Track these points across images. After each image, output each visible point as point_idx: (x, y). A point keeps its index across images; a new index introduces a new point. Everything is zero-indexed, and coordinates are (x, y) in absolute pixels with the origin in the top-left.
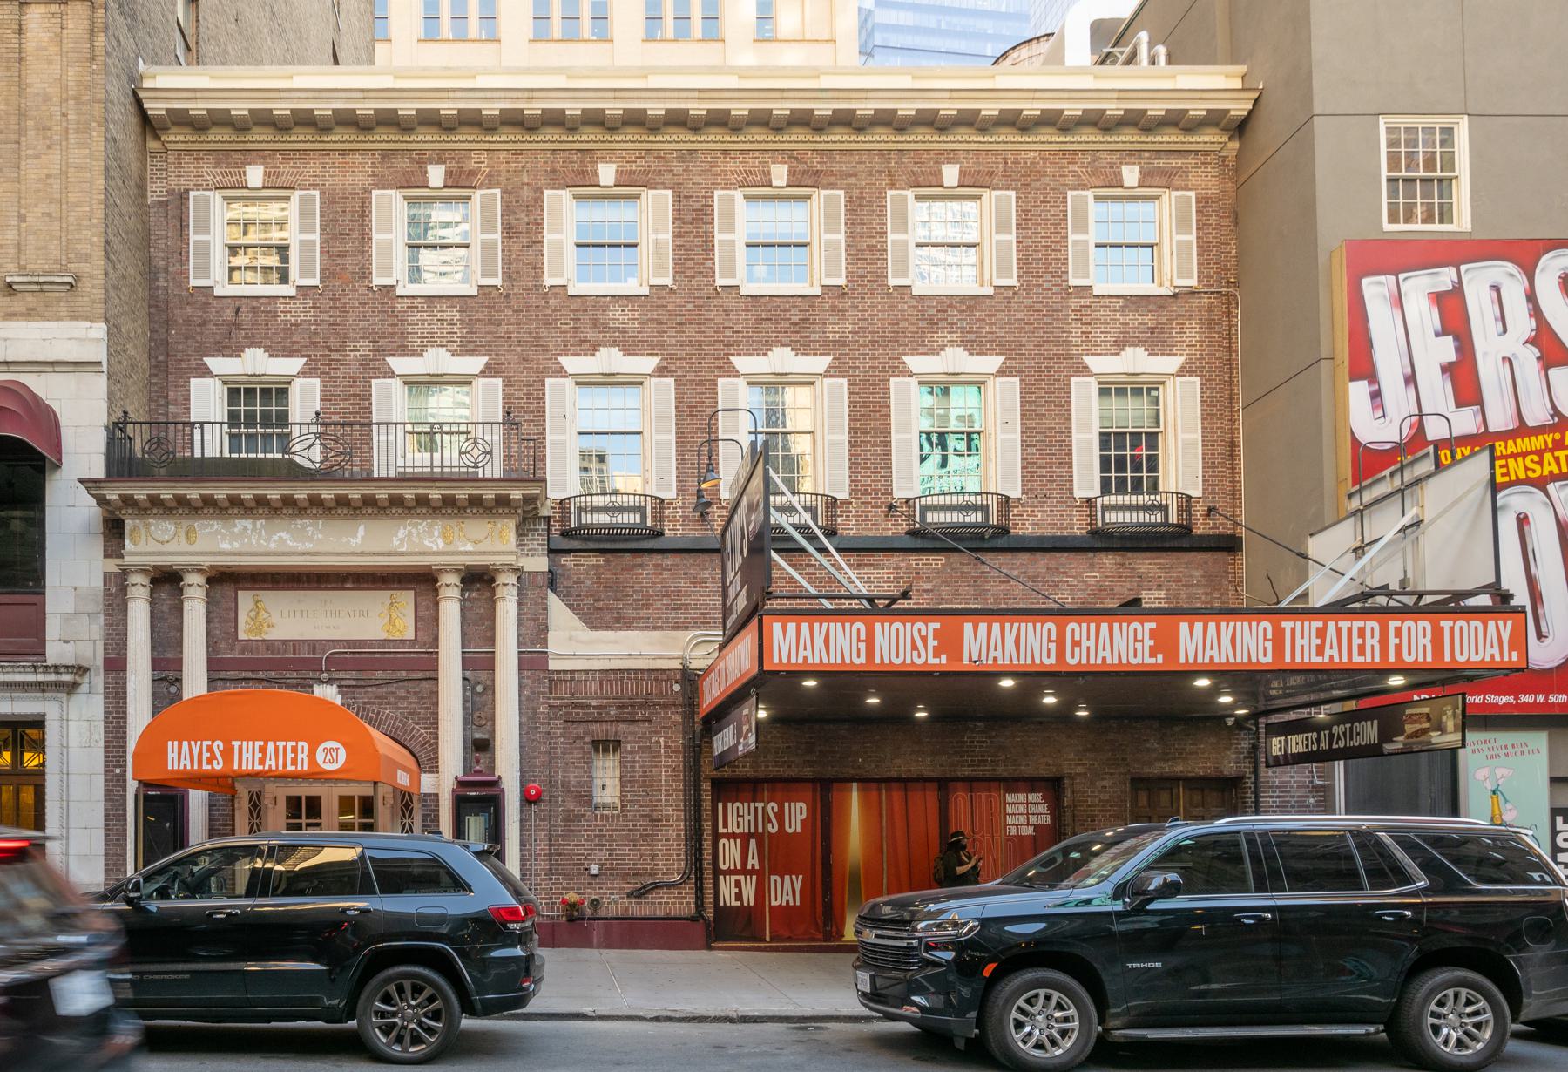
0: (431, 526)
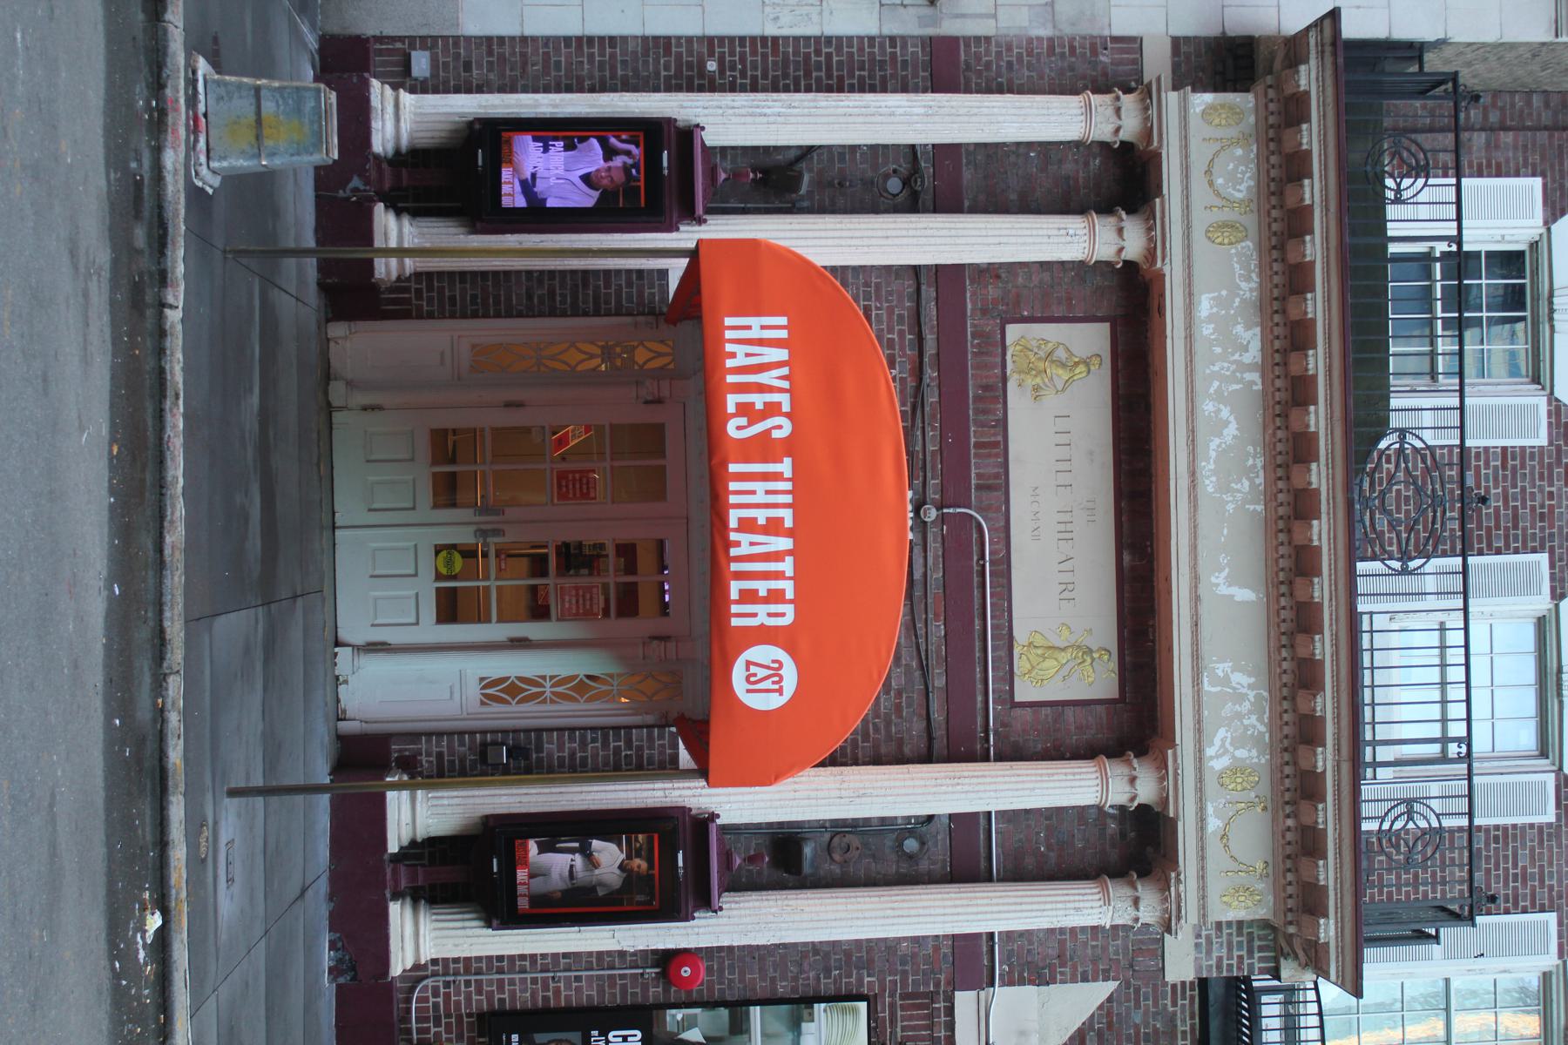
0: (1256, 741)
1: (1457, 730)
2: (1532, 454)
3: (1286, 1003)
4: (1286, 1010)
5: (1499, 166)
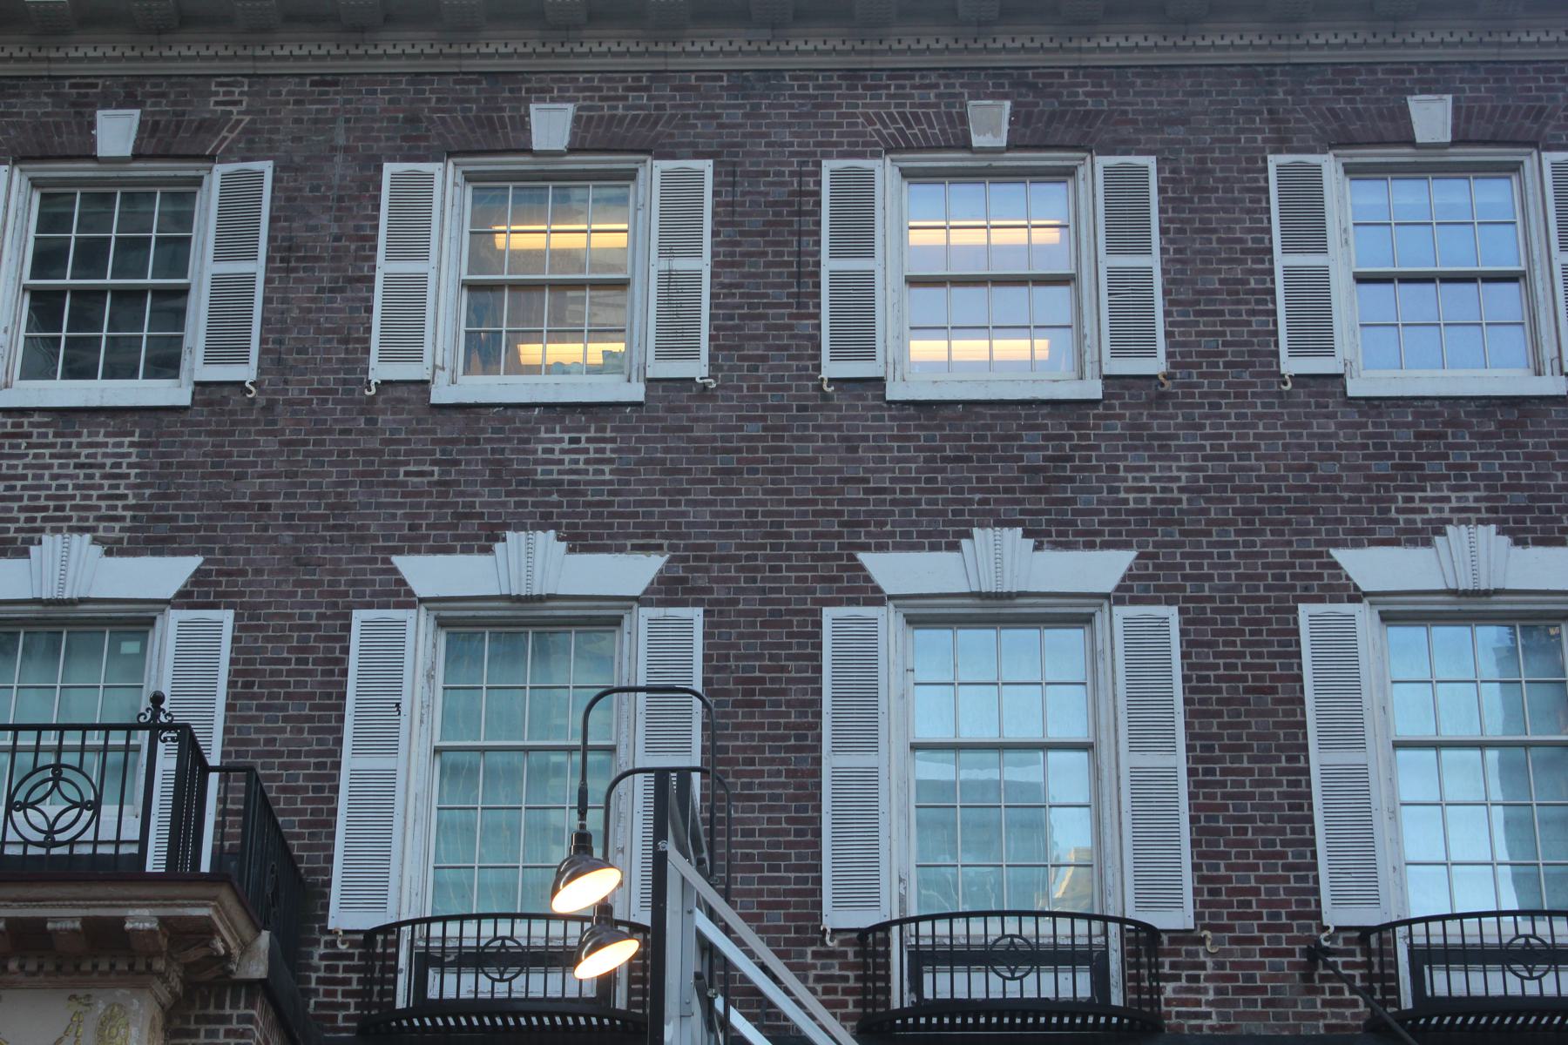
3: (441, 964)
4: (451, 964)
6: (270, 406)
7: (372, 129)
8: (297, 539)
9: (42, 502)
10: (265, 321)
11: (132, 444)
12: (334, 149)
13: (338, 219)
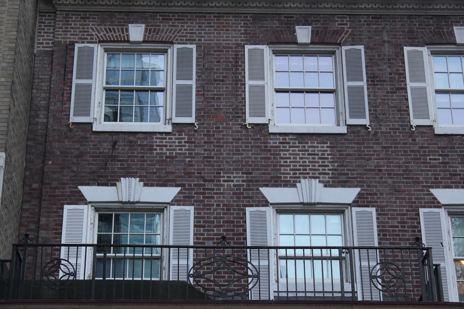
1: (335, 253)
2: (198, 213)
5: (56, 225)
6: (376, 134)
7: (397, 35)
8: (394, 182)
9: (298, 167)
10: (369, 103)
11: (327, 147)
12: (384, 42)
13: (389, 67)
